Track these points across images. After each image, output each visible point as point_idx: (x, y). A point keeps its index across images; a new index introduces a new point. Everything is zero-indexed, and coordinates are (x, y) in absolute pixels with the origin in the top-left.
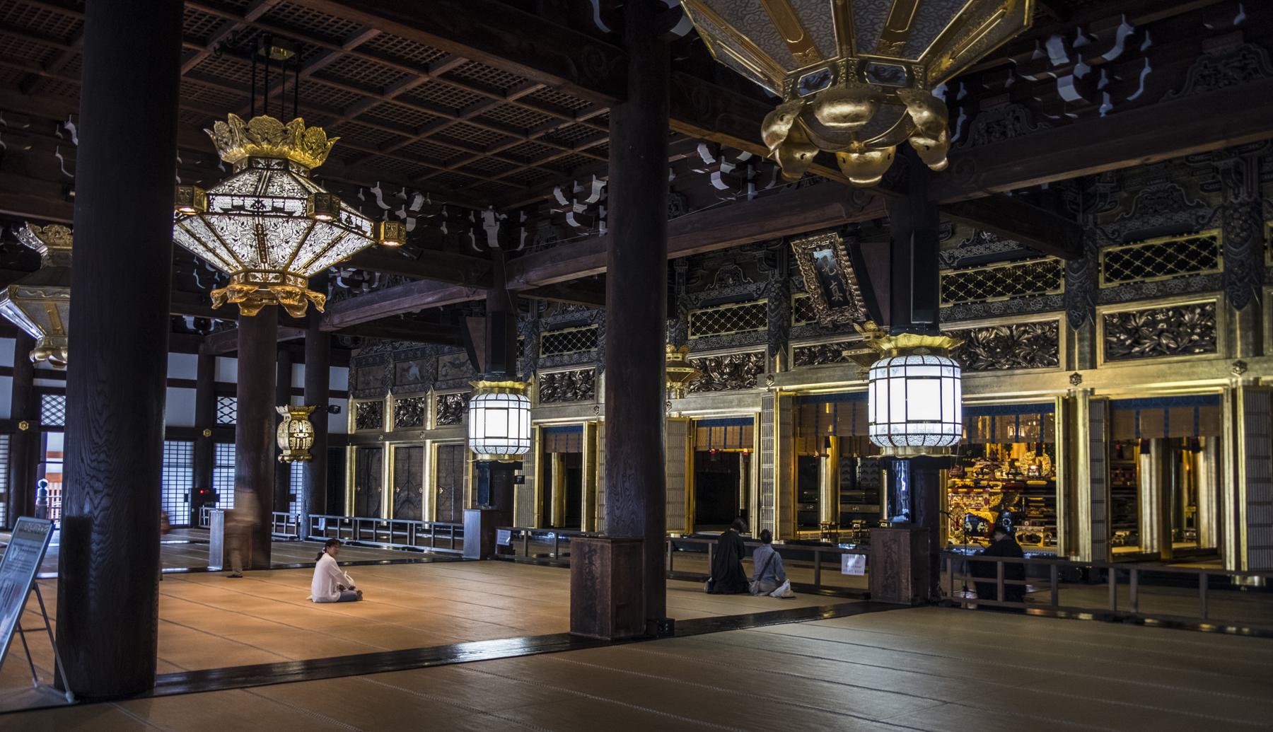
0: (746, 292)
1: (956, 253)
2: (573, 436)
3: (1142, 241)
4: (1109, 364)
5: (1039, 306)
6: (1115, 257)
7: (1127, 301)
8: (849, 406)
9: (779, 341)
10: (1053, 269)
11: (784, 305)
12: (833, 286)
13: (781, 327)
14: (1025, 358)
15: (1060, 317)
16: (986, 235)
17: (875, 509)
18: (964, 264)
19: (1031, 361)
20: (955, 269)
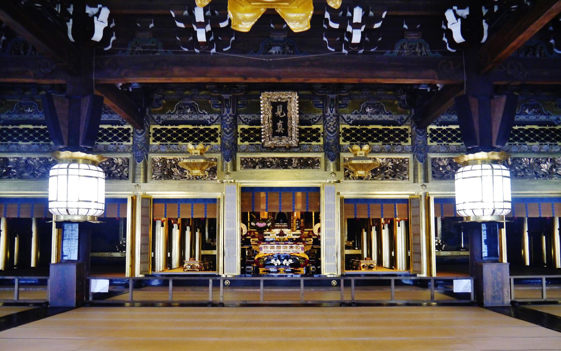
0: (201, 119)
1: (352, 117)
2: (210, 206)
3: (447, 126)
4: (434, 182)
5: (399, 150)
7: (442, 152)
8: (250, 194)
9: (230, 152)
10: (404, 131)
11: (235, 131)
12: (280, 124)
14: (390, 175)
15: (409, 156)
16: (368, 110)
17: (214, 252)
18: (356, 123)
19: (394, 176)
20: (351, 125)
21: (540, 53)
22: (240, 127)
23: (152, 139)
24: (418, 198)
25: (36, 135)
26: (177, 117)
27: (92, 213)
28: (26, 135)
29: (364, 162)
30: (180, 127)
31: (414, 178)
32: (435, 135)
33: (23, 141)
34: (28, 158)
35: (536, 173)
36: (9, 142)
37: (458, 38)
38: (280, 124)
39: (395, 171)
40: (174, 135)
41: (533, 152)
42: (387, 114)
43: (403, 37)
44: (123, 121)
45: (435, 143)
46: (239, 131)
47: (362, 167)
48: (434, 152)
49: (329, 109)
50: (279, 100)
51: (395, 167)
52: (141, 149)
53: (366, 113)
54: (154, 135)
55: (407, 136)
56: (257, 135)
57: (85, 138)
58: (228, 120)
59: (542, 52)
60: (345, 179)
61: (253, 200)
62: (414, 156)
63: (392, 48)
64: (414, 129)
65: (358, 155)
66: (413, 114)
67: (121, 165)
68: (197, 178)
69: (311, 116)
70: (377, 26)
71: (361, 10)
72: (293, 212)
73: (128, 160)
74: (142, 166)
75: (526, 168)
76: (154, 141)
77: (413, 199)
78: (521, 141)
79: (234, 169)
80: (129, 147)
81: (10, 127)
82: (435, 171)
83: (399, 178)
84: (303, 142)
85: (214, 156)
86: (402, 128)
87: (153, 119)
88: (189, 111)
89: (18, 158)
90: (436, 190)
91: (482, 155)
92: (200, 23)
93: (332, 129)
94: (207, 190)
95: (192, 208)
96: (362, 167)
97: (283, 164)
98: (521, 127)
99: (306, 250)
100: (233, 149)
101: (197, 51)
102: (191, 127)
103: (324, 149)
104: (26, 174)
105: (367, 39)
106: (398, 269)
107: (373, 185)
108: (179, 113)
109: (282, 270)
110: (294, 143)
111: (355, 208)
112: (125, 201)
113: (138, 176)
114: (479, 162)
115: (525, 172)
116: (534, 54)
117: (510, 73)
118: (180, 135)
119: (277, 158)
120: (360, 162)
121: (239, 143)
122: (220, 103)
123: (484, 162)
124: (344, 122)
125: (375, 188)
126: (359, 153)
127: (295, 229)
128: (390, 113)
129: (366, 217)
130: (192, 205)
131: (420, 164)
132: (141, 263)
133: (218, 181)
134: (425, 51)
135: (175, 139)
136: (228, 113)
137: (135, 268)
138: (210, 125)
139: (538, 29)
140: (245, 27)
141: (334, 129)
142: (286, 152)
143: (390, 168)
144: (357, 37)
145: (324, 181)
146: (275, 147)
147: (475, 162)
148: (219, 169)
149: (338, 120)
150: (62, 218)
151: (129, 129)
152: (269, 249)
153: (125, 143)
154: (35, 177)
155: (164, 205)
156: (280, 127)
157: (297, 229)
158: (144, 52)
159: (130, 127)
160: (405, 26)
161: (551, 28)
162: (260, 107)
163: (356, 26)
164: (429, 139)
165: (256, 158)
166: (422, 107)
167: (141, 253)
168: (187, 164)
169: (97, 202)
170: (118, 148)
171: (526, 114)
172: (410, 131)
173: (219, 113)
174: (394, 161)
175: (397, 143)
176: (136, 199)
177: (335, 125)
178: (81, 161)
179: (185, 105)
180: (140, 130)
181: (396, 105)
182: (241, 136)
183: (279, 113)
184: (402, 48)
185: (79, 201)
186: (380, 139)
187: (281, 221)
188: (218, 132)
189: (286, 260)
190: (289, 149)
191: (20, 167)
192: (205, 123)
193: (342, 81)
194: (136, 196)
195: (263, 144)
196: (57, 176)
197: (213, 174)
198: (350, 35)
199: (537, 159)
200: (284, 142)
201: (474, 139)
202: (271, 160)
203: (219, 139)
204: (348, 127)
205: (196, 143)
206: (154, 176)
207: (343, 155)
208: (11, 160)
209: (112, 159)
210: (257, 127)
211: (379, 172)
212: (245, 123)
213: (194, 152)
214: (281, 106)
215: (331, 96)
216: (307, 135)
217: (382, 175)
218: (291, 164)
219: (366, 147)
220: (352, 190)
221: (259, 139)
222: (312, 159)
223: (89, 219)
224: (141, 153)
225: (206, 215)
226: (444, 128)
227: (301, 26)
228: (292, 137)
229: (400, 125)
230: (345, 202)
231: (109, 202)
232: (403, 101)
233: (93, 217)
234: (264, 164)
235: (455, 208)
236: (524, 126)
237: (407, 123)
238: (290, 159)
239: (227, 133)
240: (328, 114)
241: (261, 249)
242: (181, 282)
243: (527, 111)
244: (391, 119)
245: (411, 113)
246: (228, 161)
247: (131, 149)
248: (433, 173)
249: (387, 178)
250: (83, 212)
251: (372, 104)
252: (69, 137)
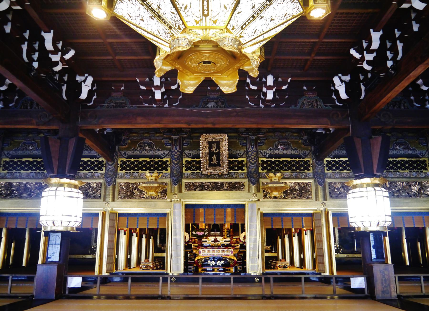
0: (156, 154)
2: (161, 219)
3: (339, 158)
4: (331, 200)
5: (304, 176)
6: (329, 162)
7: (336, 178)
8: (192, 210)
9: (177, 179)
11: (181, 163)
12: (214, 157)
13: (179, 172)
14: (298, 195)
15: (311, 181)
16: (280, 147)
17: (164, 255)
18: (271, 156)
20: (267, 158)
21: (404, 106)
22: (185, 159)
23: (119, 168)
24: (320, 213)
25: (35, 166)
26: (138, 152)
27: (72, 225)
28: (27, 166)
29: (278, 185)
30: (141, 160)
31: (316, 198)
32: (330, 165)
33: (24, 171)
34: (27, 183)
35: (408, 193)
36: (14, 171)
37: (343, 95)
38: (214, 157)
39: (301, 192)
40: (136, 166)
41: (405, 177)
42: (294, 150)
43: (304, 96)
44: (98, 155)
45: (330, 171)
46: (184, 162)
47: (276, 189)
48: (330, 178)
49: (250, 147)
50: (214, 140)
51: (301, 189)
52: (111, 176)
53: (278, 149)
54: (121, 166)
55: (309, 166)
56: (198, 166)
57: (70, 168)
58: (176, 155)
59: (406, 105)
60: (264, 198)
61: (194, 214)
62: (315, 181)
63: (296, 103)
64: (314, 160)
65: (273, 180)
66: (313, 150)
67: (96, 188)
68: (152, 198)
69: (237, 152)
70: (284, 87)
71: (273, 77)
72: (224, 224)
73: (101, 184)
74: (111, 189)
75: (401, 189)
76: (121, 170)
77: (316, 213)
78: (395, 169)
79: (180, 191)
80: (102, 174)
81: (16, 160)
82: (332, 192)
83: (304, 197)
84: (232, 171)
85: (165, 181)
86: (305, 160)
87: (121, 154)
88: (147, 148)
89: (20, 183)
90: (333, 206)
91: (367, 180)
92: (157, 86)
93: (253, 161)
94: (159, 207)
95: (148, 221)
96: (276, 189)
97: (217, 187)
98: (394, 159)
99: (235, 253)
100: (179, 176)
101: (154, 105)
102: (148, 160)
104: (24, 195)
105: (277, 97)
106: (307, 268)
107: (285, 203)
108: (140, 150)
109: (216, 269)
110: (225, 171)
111: (272, 221)
112: (97, 215)
113: (107, 196)
114: (365, 186)
115: (400, 193)
116: (400, 107)
117: (383, 120)
118: (140, 166)
119: (212, 182)
120: (275, 185)
121: (184, 171)
122: (170, 142)
123: (368, 185)
125: (287, 205)
126: (273, 179)
127: (226, 237)
128: (296, 149)
129: (281, 227)
131: (320, 188)
132: (107, 263)
133: (168, 200)
134: (320, 105)
135: (136, 168)
136: (176, 149)
137: (102, 268)
138: (162, 158)
139: (401, 90)
140: (190, 90)
142: (219, 178)
143: (297, 190)
144: (270, 96)
145: (248, 200)
146: (211, 175)
147: (361, 185)
148: (169, 191)
149: (257, 154)
150: (49, 229)
151: (103, 161)
152: (206, 253)
153: (99, 171)
154: (31, 196)
155: (126, 218)
157: (228, 237)
158: (116, 107)
159: (103, 159)
160: (305, 88)
161: (410, 89)
162: (200, 145)
163: (270, 88)
164: (326, 168)
165: (196, 183)
166: (319, 144)
167: (108, 256)
168: (145, 187)
169: (76, 216)
170: (94, 175)
171: (397, 149)
172: (311, 162)
173: (170, 149)
174: (300, 184)
175: (302, 171)
176: (105, 214)
177: (255, 158)
178: (66, 185)
179: (145, 144)
180: (111, 162)
181: (300, 143)
182: (186, 166)
183: (214, 149)
184: (303, 103)
185: (63, 215)
186: (289, 168)
187: (215, 230)
188: (168, 163)
189: (219, 261)
190: (221, 176)
191: (20, 190)
192: (159, 157)
193: (260, 126)
194: (106, 212)
195: (202, 172)
196: (48, 196)
197: (164, 195)
198: (265, 94)
199: (408, 183)
200: (217, 170)
201: (359, 167)
202: (208, 184)
203: (169, 169)
204: (265, 159)
205: (152, 171)
206: (120, 196)
207: (262, 180)
208: (14, 184)
209: (89, 184)
210: (197, 160)
211: (289, 193)
212: (189, 157)
213: (150, 178)
214: (215, 144)
215: (251, 137)
216: (235, 166)
217: (292, 195)
219: (279, 175)
220: (269, 207)
221: (199, 168)
222: (239, 183)
223: (69, 229)
224: (111, 179)
225: (158, 226)
226: (337, 160)
227: (230, 89)
228: (223, 167)
229: (304, 158)
230: (264, 216)
231: (86, 215)
232: (305, 140)
233: (72, 228)
234: (202, 187)
235: (348, 220)
236: (397, 158)
237: (309, 156)
238: (222, 184)
239: (176, 164)
240: (250, 150)
241: (200, 252)
242: (138, 279)
243: (398, 147)
244: (297, 154)
245: (311, 150)
246: (175, 185)
247: (104, 176)
248: (330, 193)
249: (295, 197)
250: (65, 224)
251: (282, 143)
252: (59, 167)
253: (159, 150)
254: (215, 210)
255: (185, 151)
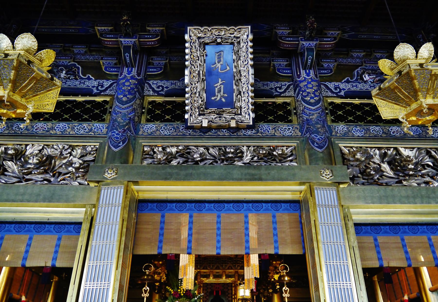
1: (342, 86)
16: (366, 77)
49: (303, 72)
58: (127, 84)
61: (162, 229)
72: (248, 254)
93: (312, 98)
100: (129, 129)
103: (301, 131)
111: (377, 246)
124: (330, 94)
130: (31, 239)
141: (316, 98)
143: (428, 166)
156: (219, 91)
177: (317, 94)
218: (241, 158)
239: (123, 103)
251: (372, 70)
253: (89, 79)
254: (219, 217)
255: (151, 82)
